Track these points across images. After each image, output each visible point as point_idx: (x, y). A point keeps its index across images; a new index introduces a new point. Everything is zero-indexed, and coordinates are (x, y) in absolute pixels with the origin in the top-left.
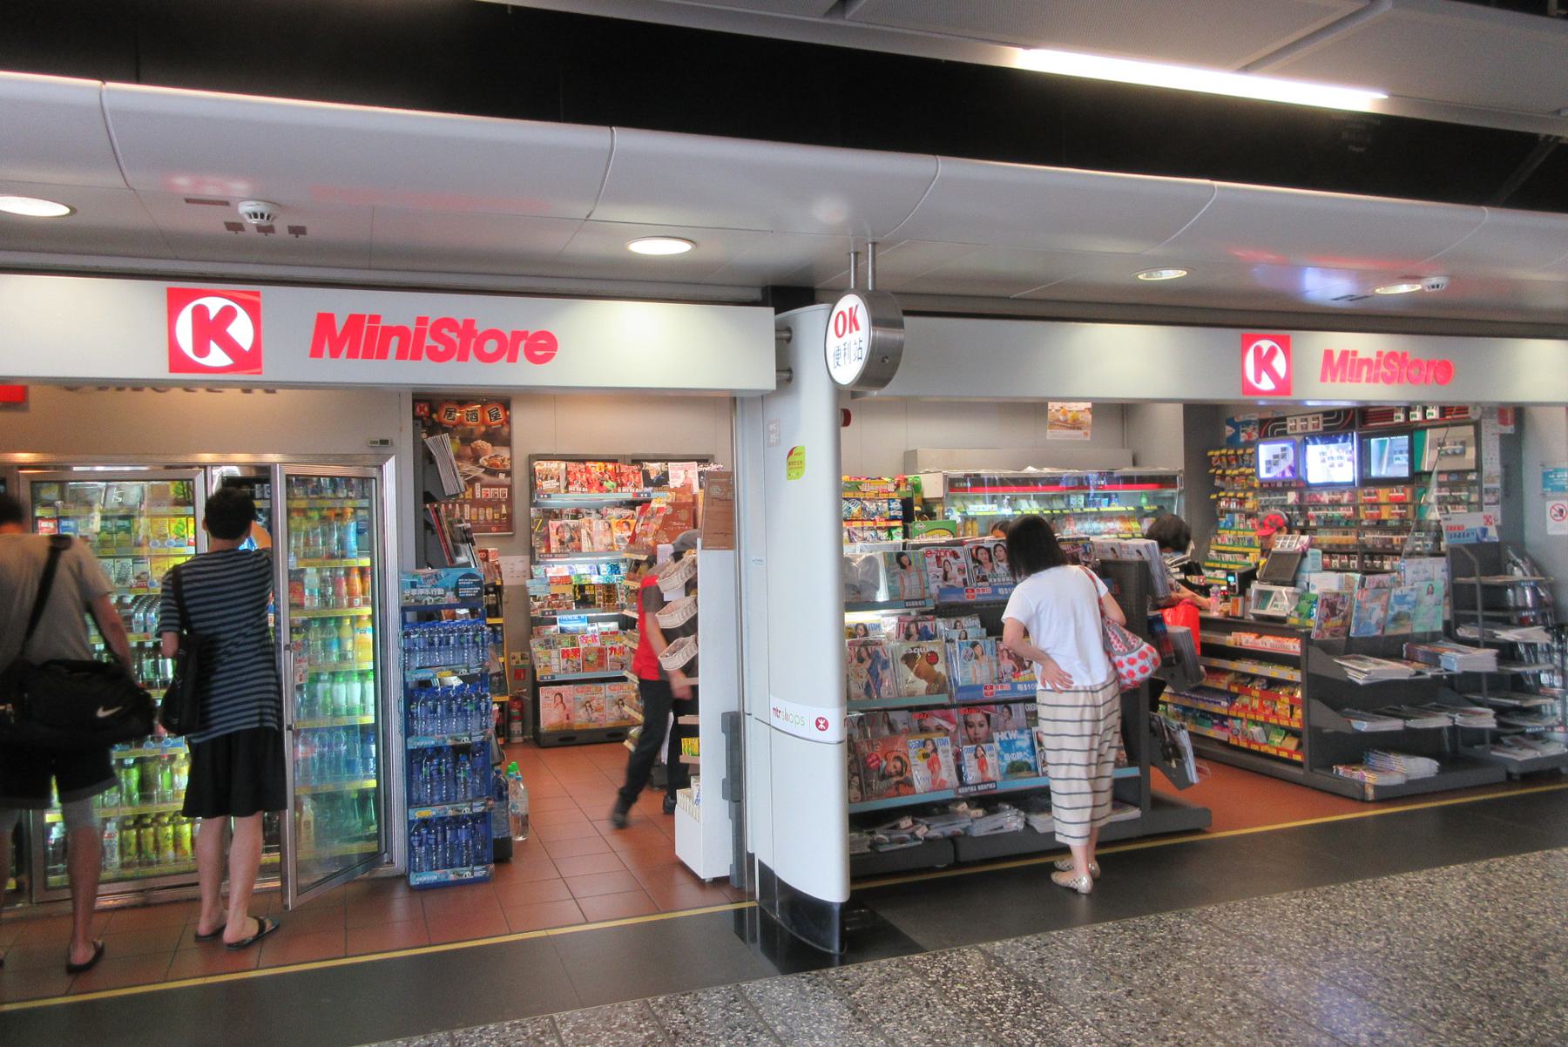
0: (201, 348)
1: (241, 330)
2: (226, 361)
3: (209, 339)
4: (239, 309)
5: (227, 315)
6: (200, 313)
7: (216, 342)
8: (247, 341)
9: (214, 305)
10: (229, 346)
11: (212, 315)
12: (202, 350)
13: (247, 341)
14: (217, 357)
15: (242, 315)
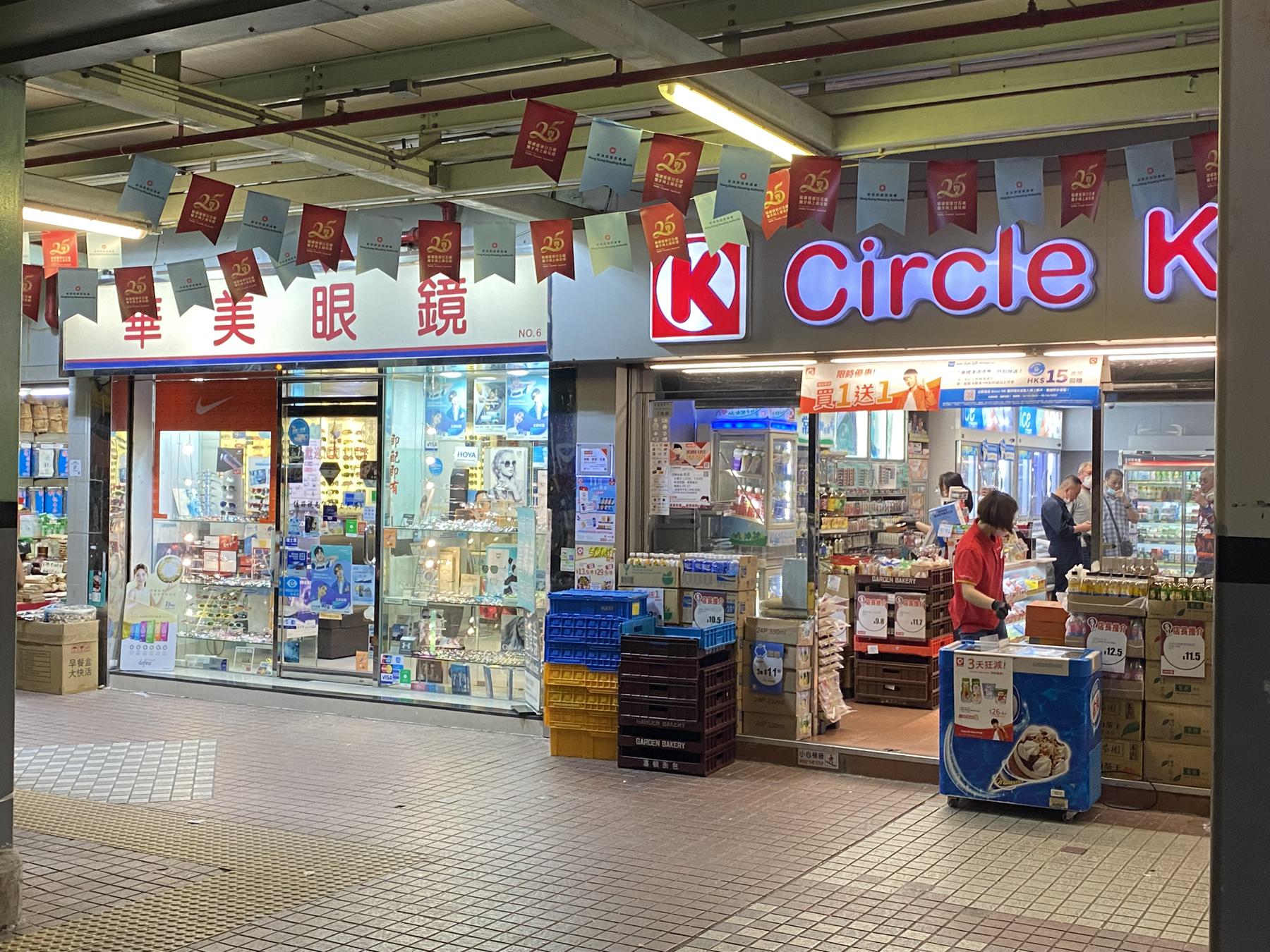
2: (705, 323)
3: (691, 297)
10: (711, 305)
12: (681, 313)
14: (697, 320)
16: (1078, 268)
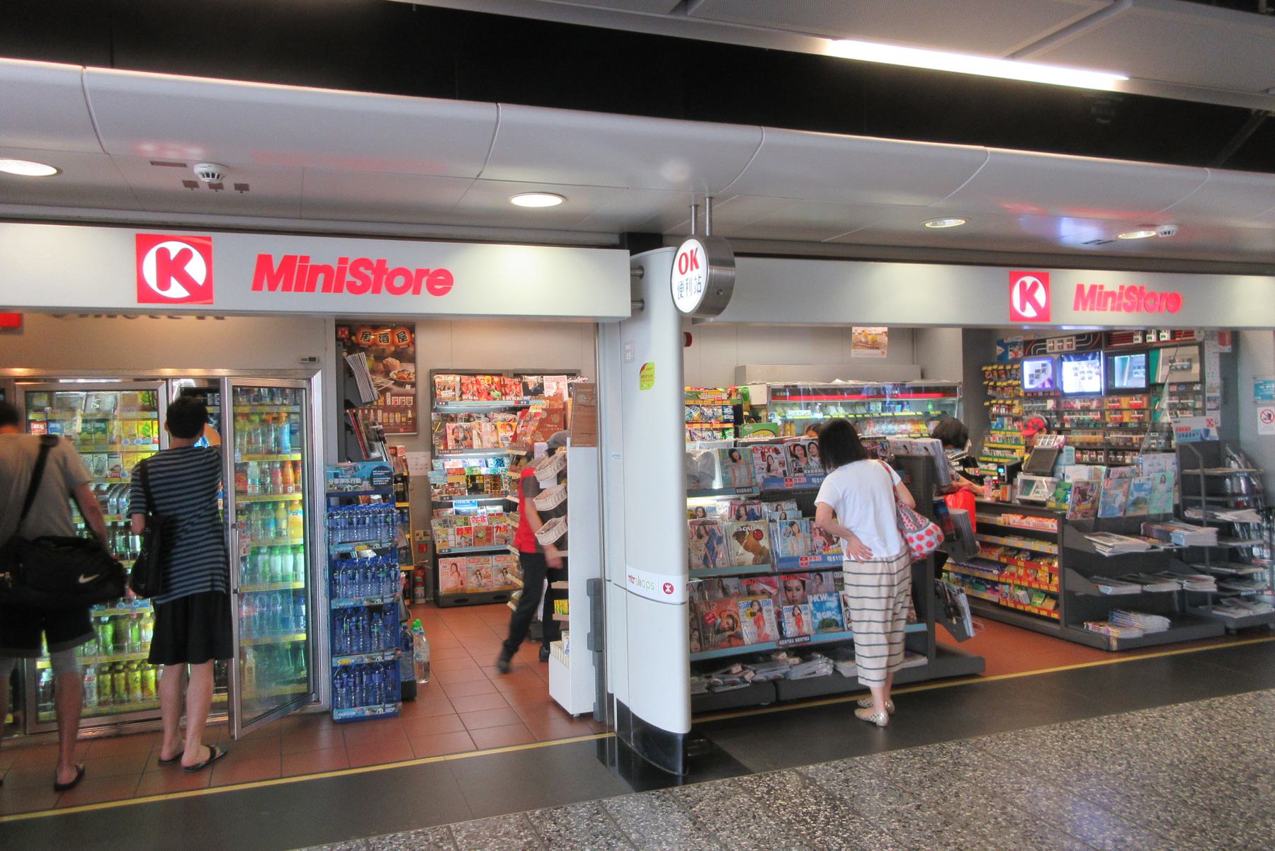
0: (164, 283)
1: (196, 268)
2: (184, 293)
3: (170, 275)
4: (194, 251)
5: (185, 256)
6: (163, 254)
7: (176, 278)
8: (201, 277)
9: (174, 248)
10: (186, 281)
11: (173, 256)
12: (164, 284)
13: (201, 277)
14: (176, 290)
15: (197, 256)
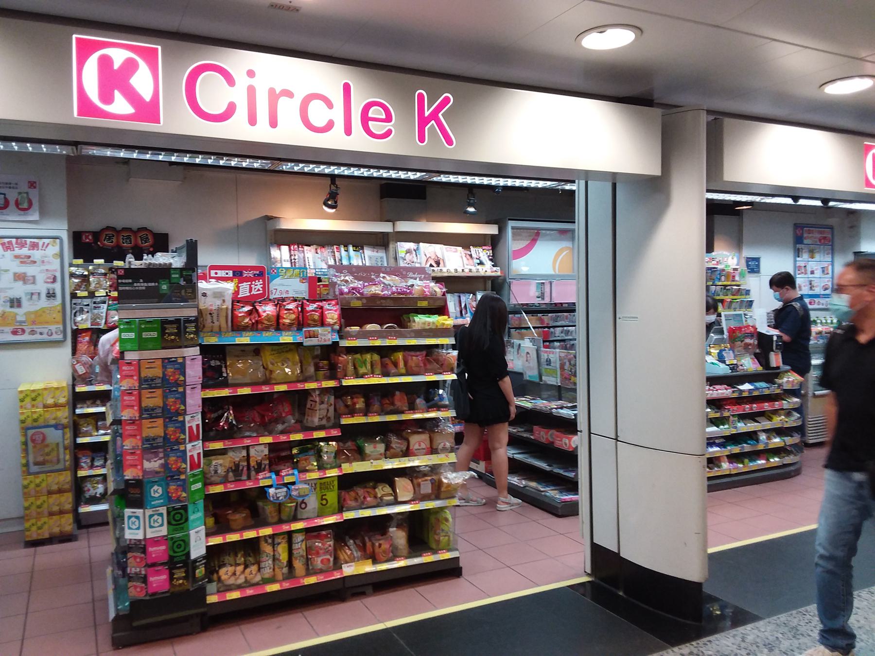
2: (128, 109)
5: (130, 67)
6: (105, 63)
10: (132, 96)
11: (116, 66)
12: (107, 98)
13: (147, 95)
14: (120, 105)
15: (143, 66)
16: (388, 119)
